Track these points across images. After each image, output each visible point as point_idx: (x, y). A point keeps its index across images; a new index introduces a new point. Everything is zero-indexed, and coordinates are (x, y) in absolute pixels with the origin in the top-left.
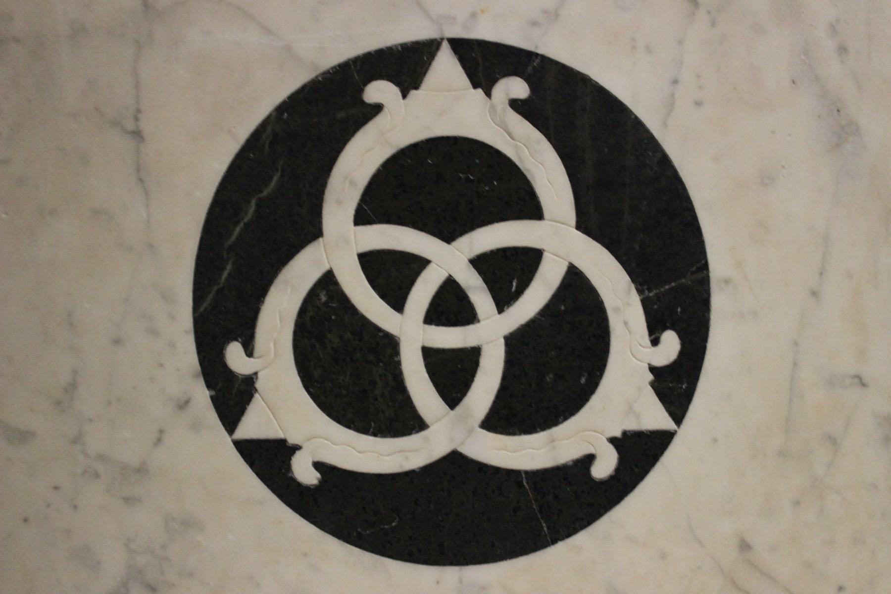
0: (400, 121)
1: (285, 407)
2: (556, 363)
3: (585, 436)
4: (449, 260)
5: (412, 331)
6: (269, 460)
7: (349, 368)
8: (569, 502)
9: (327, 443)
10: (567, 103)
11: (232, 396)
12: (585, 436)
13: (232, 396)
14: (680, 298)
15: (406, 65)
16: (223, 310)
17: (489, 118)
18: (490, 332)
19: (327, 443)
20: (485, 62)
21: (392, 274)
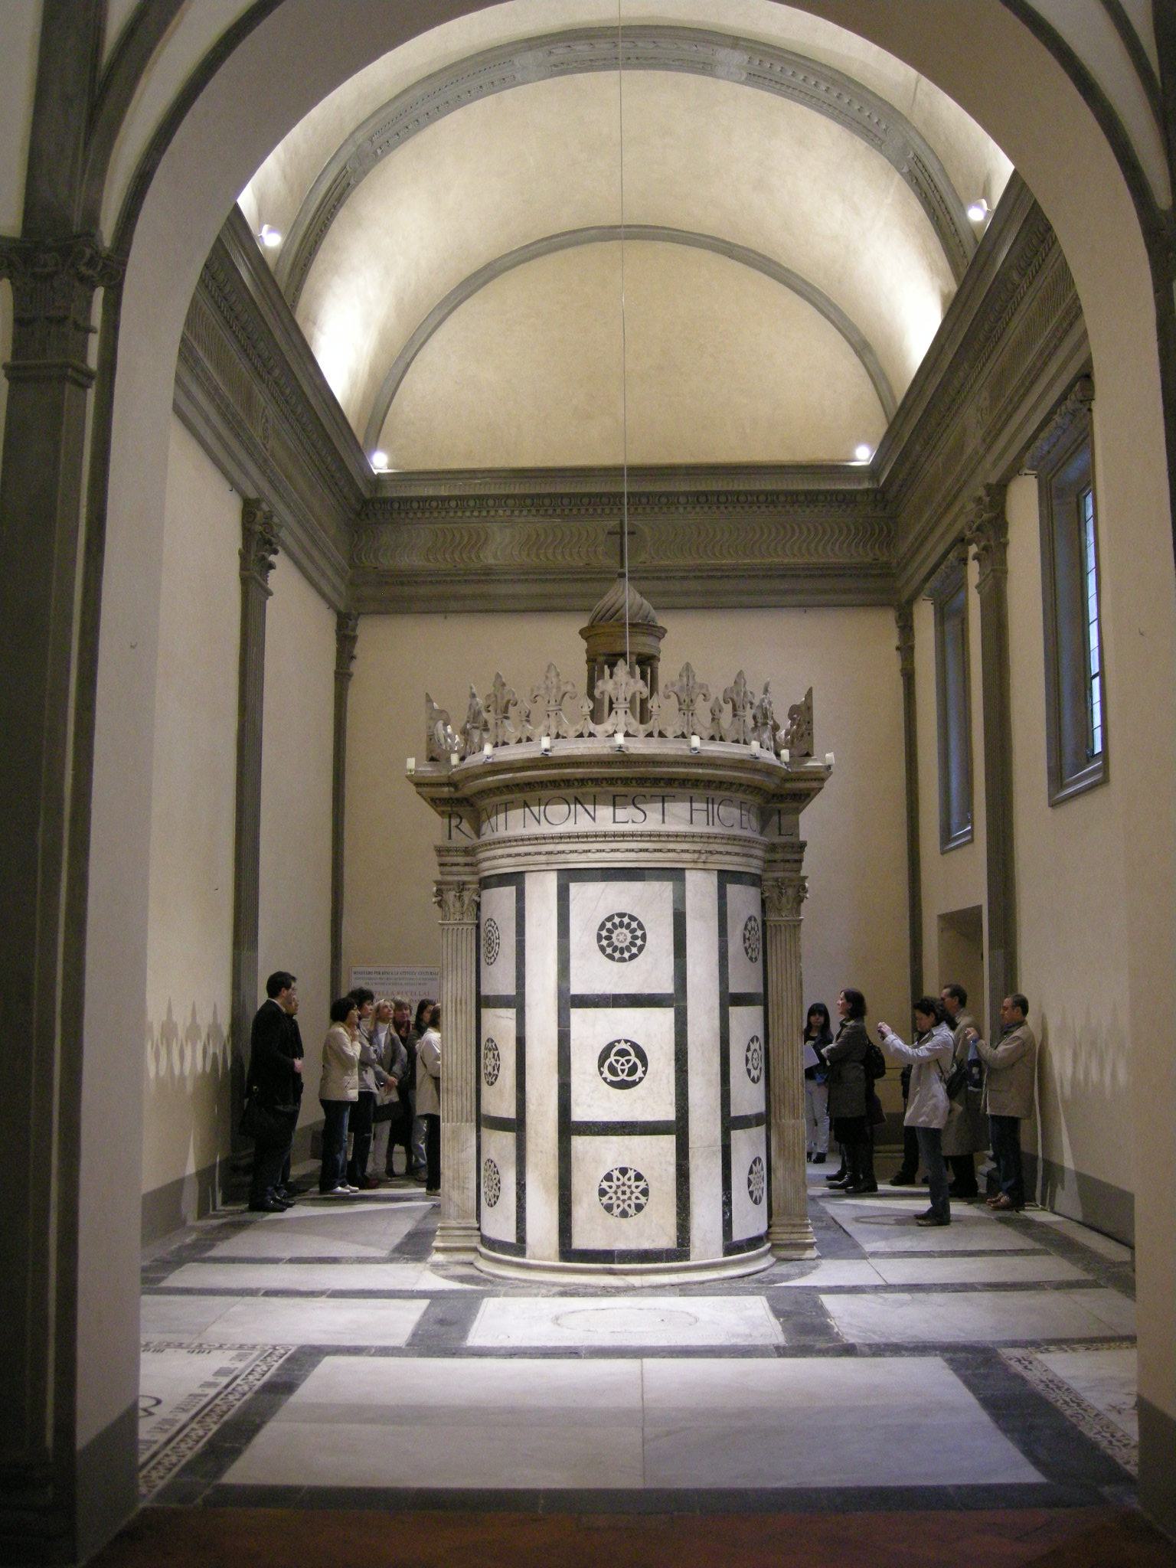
0: (618, 1047)
1: (607, 1074)
2: (633, 1070)
3: (635, 1077)
4: (623, 1060)
5: (619, 1067)
6: (605, 1079)
7: (613, 1070)
8: (634, 1084)
9: (611, 1078)
10: (634, 1045)
11: (601, 1073)
12: (635, 1077)
13: (601, 1073)
14: (645, 1064)
15: (619, 1041)
16: (601, 1065)
17: (627, 1047)
18: (626, 1067)
19: (611, 1078)
20: (626, 1041)
21: (617, 1061)
